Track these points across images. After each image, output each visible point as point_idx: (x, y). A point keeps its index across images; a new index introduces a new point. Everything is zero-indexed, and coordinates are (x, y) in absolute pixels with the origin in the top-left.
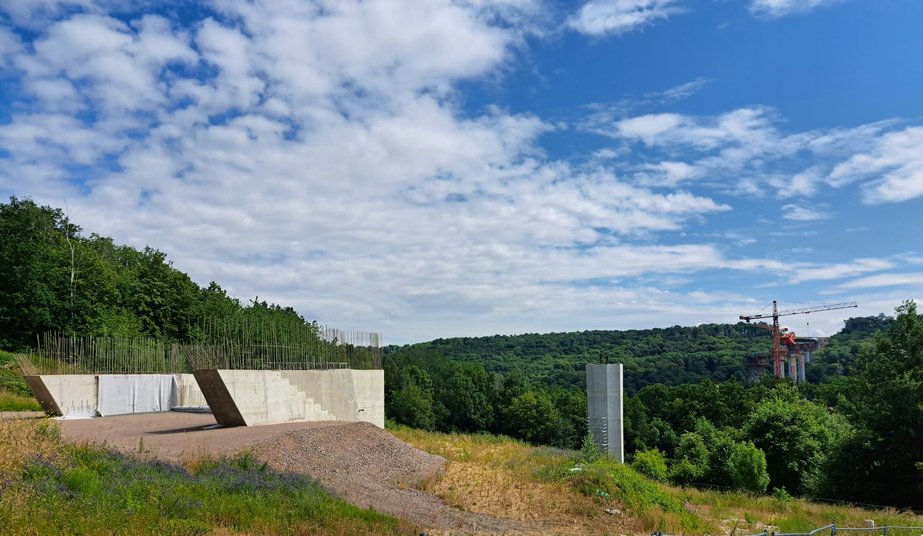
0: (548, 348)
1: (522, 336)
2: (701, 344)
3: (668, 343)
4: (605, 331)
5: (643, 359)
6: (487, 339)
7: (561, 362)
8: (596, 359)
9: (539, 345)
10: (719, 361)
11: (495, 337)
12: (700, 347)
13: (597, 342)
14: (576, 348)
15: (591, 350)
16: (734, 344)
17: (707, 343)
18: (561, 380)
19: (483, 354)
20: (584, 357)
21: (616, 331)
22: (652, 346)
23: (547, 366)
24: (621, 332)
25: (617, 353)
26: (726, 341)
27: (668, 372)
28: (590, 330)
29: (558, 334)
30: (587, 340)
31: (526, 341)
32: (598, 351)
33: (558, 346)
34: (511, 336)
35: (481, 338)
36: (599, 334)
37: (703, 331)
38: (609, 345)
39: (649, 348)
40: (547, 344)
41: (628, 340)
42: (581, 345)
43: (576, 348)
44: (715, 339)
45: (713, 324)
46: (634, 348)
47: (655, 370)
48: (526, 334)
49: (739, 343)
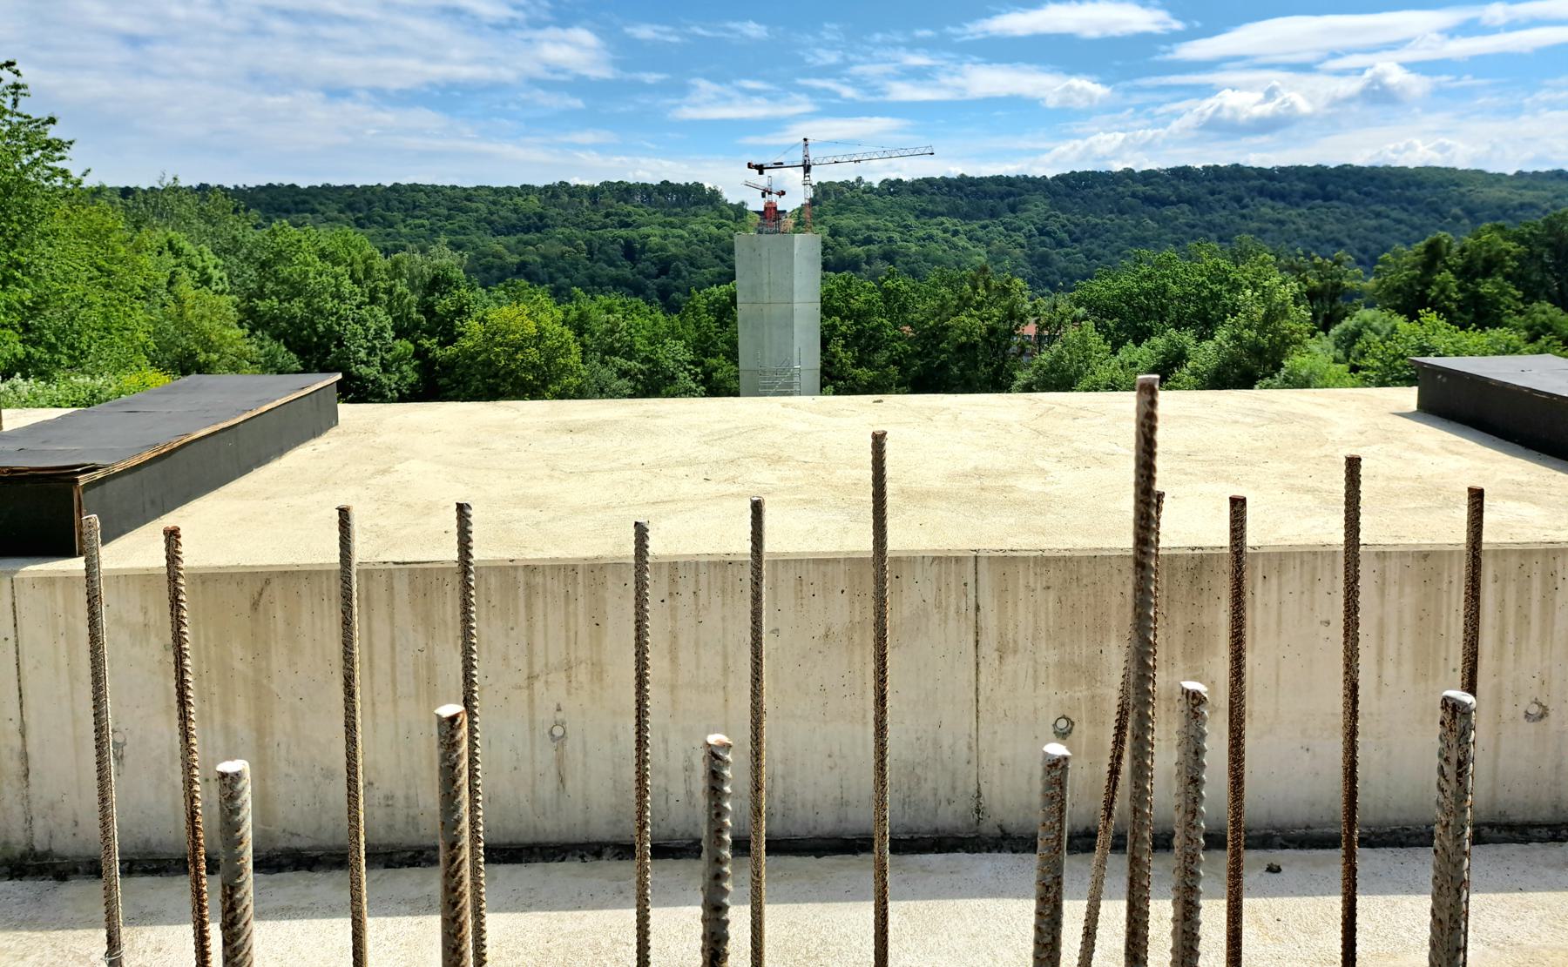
0: (323, 214)
1: (260, 189)
2: (607, 215)
3: (552, 212)
4: (434, 186)
5: (512, 240)
8: (423, 237)
9: (301, 207)
10: (644, 245)
12: (607, 220)
13: (419, 206)
14: (382, 217)
15: (409, 221)
16: (660, 217)
17: (616, 214)
20: (399, 233)
21: (454, 188)
22: (525, 215)
24: (465, 190)
25: (464, 228)
26: (646, 211)
27: (561, 263)
29: (339, 188)
30: (400, 202)
31: (272, 198)
32: (426, 222)
34: (236, 187)
36: (421, 190)
37: (607, 193)
38: (446, 212)
39: (520, 220)
40: (318, 207)
41: (479, 205)
42: (389, 209)
43: (382, 217)
44: (630, 208)
45: (622, 182)
46: (492, 218)
47: (538, 259)
48: (270, 186)
49: (669, 216)
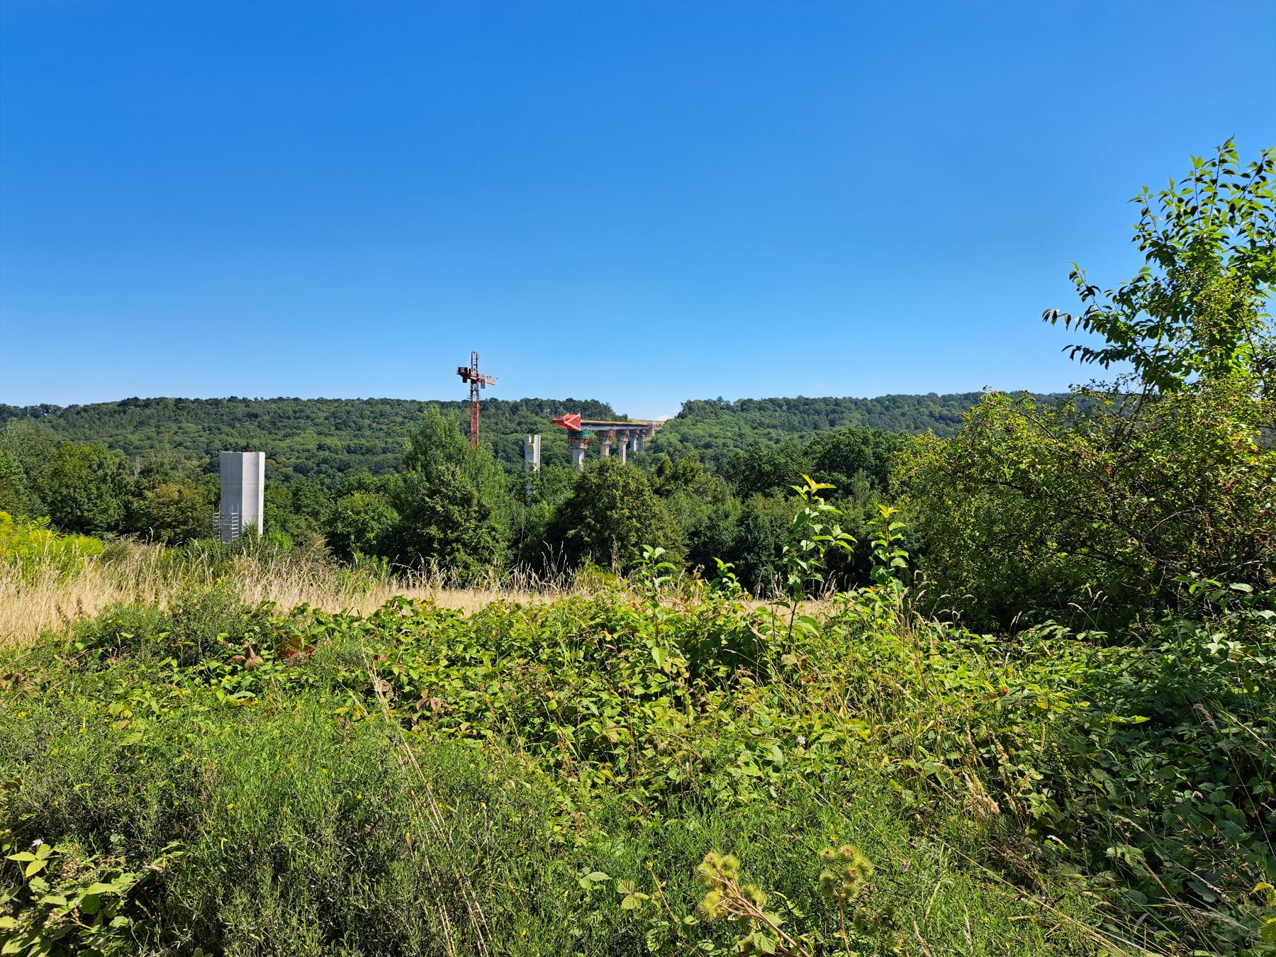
1: (273, 401)
2: (519, 424)
4: (398, 401)
6: (215, 403)
7: (328, 441)
11: (229, 400)
14: (354, 422)
18: (324, 467)
19: (206, 425)
23: (306, 447)
24: (420, 403)
28: (376, 398)
32: (384, 427)
33: (326, 418)
34: (256, 399)
35: (206, 401)
37: (524, 407)
48: (280, 399)
